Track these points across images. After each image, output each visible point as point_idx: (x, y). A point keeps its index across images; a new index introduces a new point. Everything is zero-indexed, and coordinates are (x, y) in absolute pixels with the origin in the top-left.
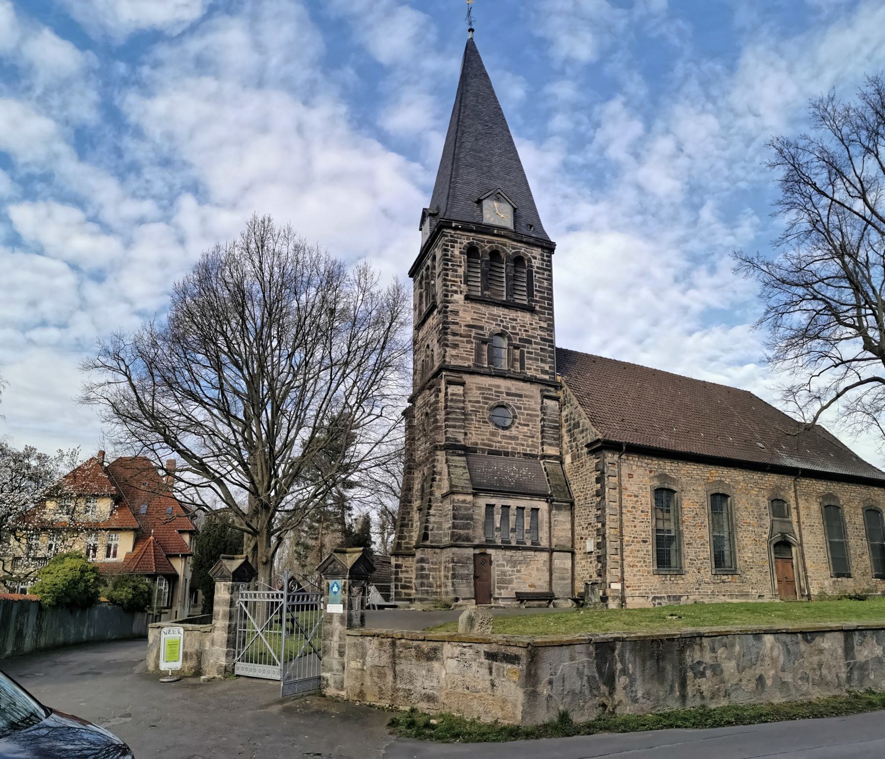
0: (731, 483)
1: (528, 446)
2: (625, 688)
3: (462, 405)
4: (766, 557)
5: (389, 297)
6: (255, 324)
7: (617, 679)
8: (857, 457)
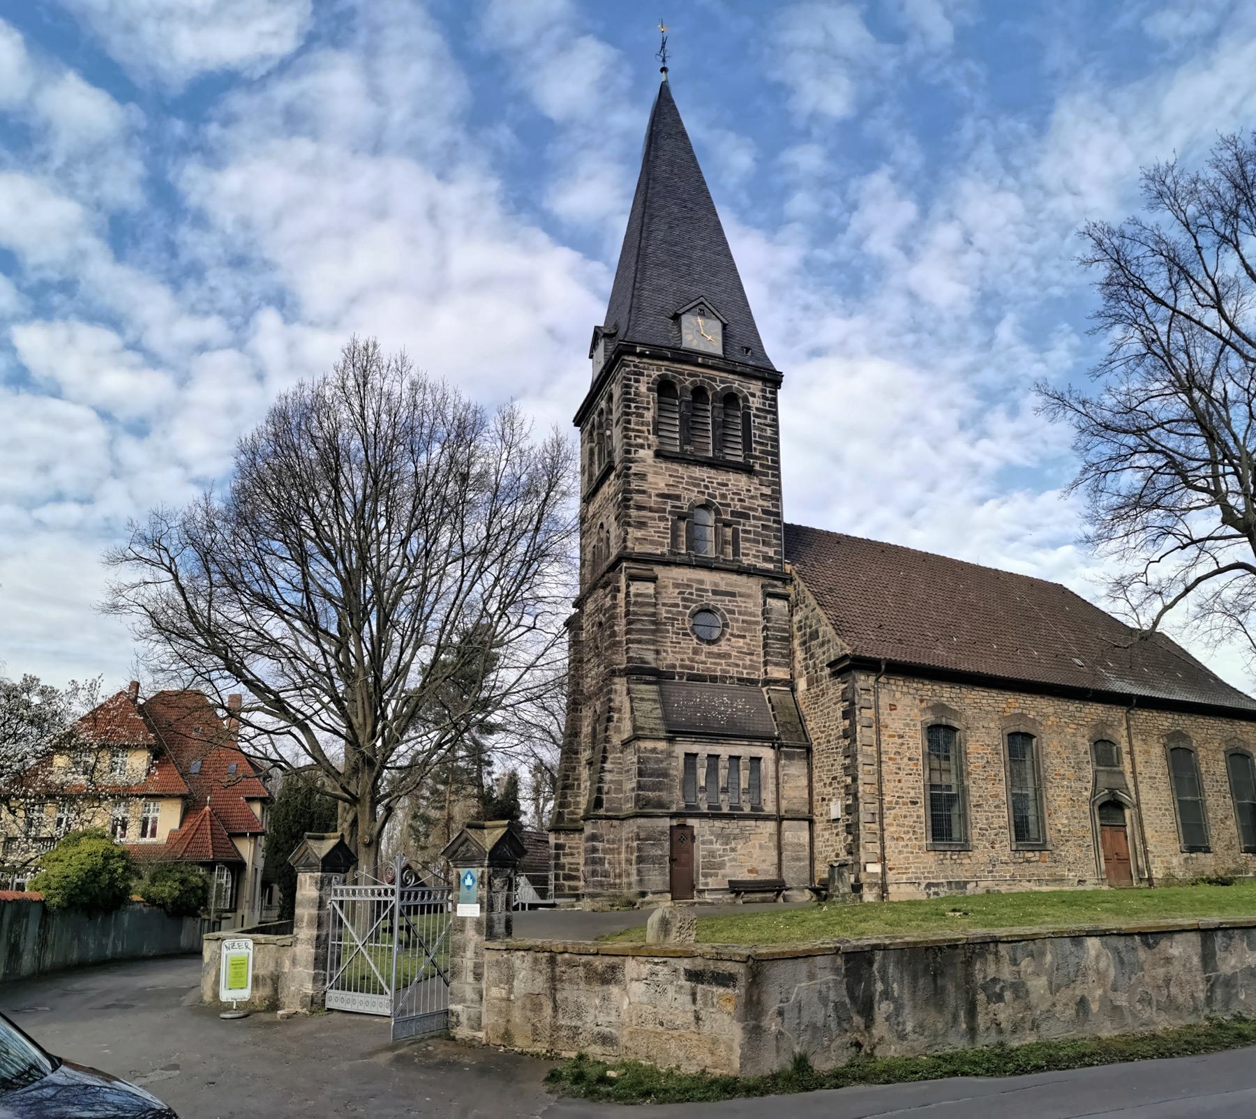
0: (1037, 718)
1: (745, 668)
2: (887, 1019)
3: (652, 610)
4: (1088, 823)
5: (546, 454)
6: (354, 496)
7: (876, 1006)
8: (1215, 678)
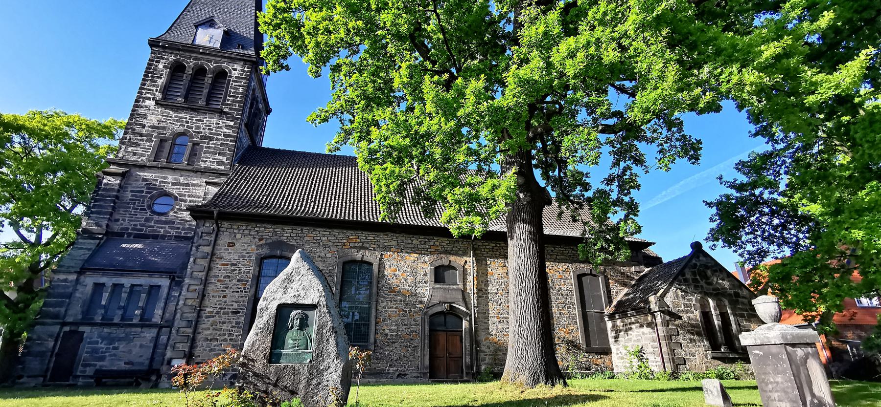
1: (183, 229)
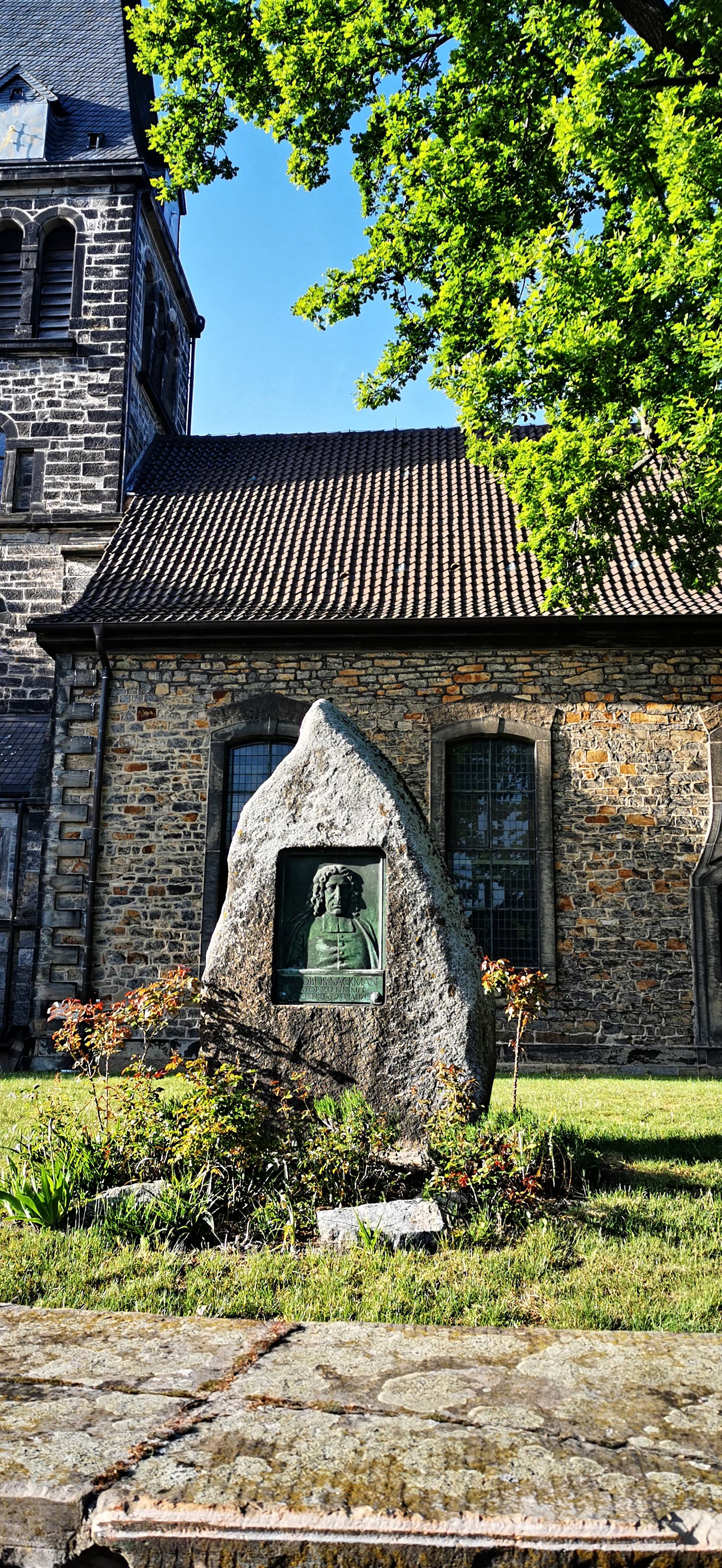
1: (29, 683)
